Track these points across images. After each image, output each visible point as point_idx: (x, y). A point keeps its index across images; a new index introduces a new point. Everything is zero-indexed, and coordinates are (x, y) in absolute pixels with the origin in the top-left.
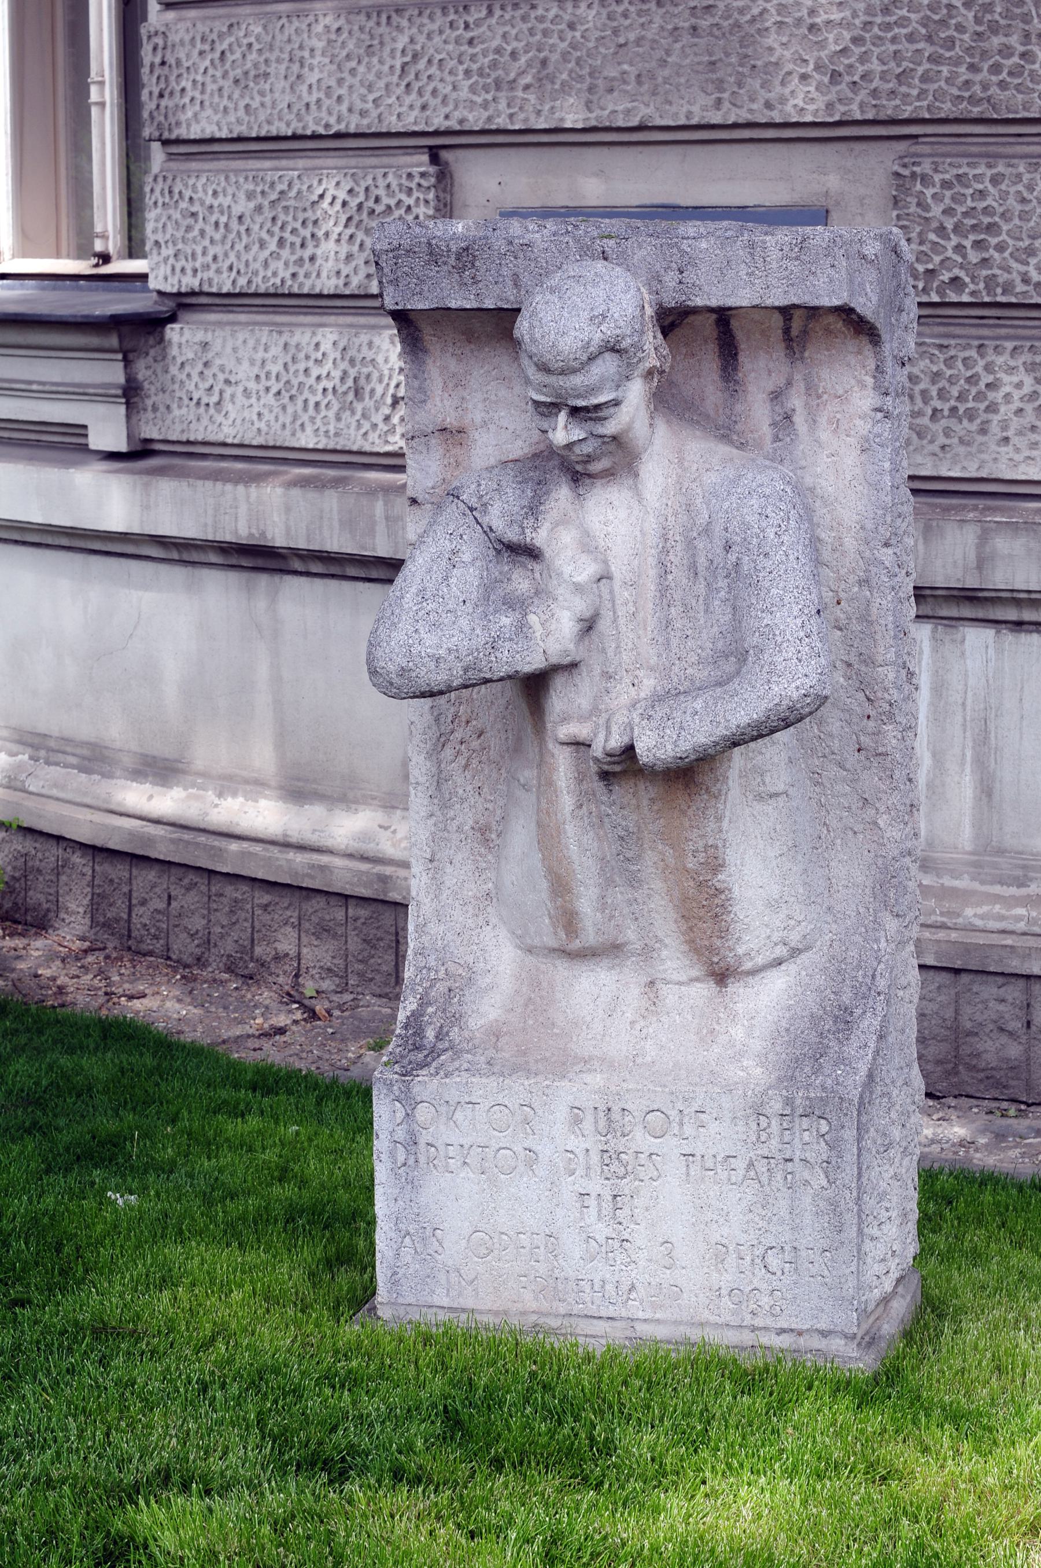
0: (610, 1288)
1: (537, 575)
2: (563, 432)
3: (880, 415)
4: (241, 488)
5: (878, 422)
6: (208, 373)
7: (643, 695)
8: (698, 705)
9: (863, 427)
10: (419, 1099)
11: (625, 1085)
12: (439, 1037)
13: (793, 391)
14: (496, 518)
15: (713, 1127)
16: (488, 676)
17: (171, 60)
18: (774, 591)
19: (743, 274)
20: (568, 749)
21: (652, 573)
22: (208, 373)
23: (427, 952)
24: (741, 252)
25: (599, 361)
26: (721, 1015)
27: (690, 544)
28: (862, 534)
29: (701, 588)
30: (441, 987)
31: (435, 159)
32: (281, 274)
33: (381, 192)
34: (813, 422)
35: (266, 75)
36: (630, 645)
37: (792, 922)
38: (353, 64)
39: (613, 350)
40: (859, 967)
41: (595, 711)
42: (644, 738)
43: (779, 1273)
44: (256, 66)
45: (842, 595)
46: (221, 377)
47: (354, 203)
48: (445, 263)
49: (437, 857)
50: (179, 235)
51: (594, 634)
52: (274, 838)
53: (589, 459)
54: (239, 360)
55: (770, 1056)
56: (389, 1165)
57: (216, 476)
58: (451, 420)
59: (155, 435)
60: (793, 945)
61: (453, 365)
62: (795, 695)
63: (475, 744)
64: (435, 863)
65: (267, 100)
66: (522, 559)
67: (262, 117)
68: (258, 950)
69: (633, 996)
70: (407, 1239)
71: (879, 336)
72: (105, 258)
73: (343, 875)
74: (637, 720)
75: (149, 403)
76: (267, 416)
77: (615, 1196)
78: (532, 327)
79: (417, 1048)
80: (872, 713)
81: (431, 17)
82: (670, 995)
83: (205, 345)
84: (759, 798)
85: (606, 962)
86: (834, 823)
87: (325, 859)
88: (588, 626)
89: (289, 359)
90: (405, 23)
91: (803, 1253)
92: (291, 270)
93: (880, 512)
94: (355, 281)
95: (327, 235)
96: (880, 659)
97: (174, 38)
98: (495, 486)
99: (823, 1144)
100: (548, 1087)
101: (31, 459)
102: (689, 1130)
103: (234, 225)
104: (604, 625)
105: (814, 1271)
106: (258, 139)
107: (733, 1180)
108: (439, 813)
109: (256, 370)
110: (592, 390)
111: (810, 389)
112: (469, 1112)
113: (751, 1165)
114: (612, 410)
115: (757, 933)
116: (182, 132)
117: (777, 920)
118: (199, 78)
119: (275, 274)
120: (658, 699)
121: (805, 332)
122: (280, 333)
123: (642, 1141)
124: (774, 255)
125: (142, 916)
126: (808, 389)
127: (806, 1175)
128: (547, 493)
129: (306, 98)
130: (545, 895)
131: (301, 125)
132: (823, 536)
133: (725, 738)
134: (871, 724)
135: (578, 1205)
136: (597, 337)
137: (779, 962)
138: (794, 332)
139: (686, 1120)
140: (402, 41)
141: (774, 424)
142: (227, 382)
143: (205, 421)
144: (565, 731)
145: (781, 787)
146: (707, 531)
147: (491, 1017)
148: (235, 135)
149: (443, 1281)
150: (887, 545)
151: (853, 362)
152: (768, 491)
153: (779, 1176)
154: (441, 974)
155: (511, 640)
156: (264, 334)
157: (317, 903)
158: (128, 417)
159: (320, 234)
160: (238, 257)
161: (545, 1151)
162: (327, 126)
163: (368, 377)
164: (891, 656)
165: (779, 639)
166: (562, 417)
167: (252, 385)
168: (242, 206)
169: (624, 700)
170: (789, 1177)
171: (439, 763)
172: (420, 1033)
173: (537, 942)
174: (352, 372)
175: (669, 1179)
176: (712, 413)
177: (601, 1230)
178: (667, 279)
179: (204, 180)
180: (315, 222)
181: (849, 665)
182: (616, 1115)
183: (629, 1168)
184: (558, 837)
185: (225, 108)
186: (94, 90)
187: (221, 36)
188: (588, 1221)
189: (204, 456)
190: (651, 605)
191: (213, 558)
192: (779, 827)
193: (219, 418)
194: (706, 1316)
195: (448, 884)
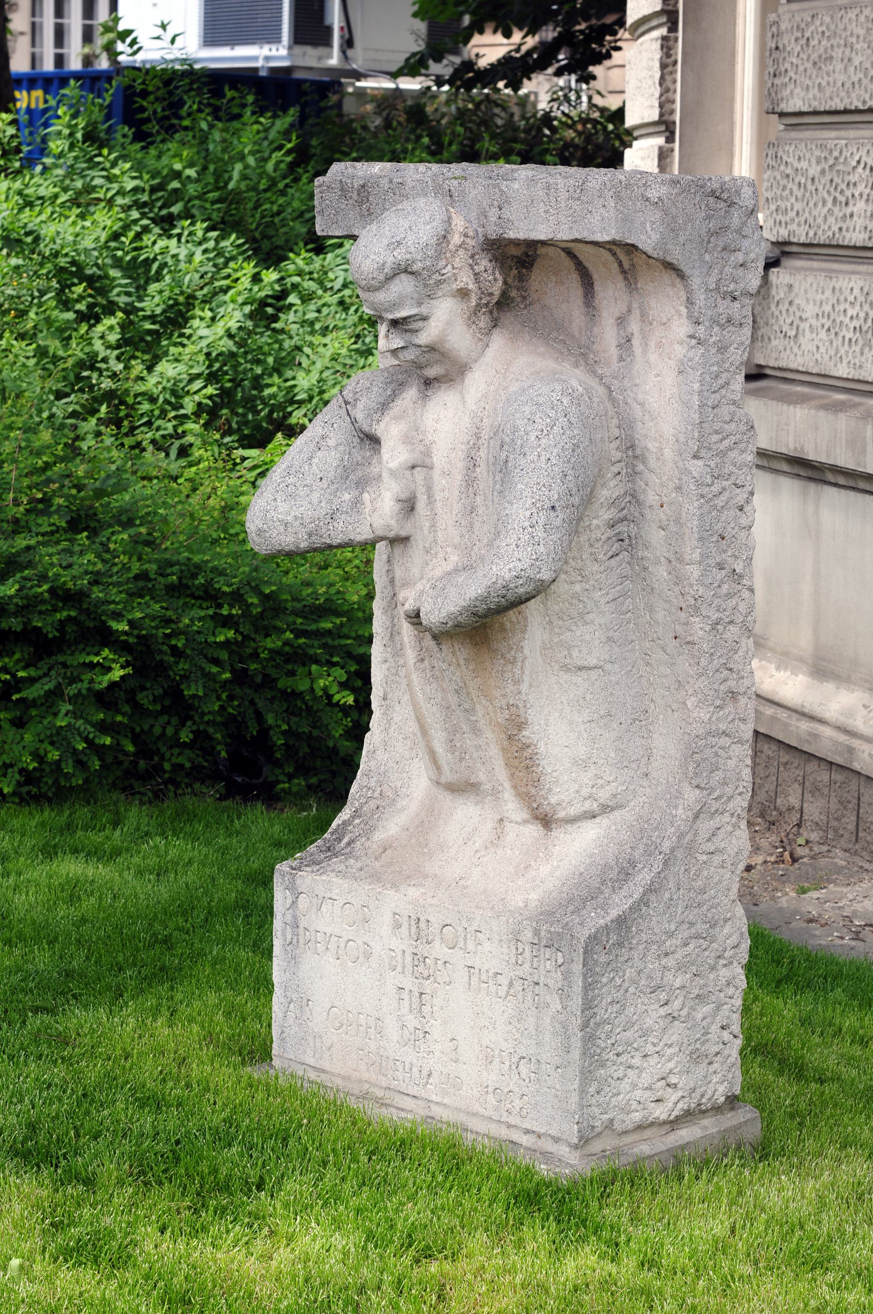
0: (415, 1070)
3: (694, 341)
5: (692, 347)
9: (680, 351)
15: (487, 945)
16: (328, 541)
18: (520, 486)
21: (460, 465)
23: (372, 774)
24: (540, 192)
25: (397, 281)
26: (541, 854)
30: (372, 804)
37: (600, 782)
39: (406, 271)
43: (527, 1080)
44: (826, 50)
45: (665, 499)
49: (389, 697)
52: (796, 708)
54: (808, 300)
60: (601, 801)
62: (507, 576)
64: (388, 702)
73: (827, 742)
76: (822, 350)
80: (684, 606)
84: (565, 668)
88: (409, 506)
89: (835, 302)
91: (543, 1066)
92: (839, 225)
93: (690, 428)
96: (687, 557)
100: (380, 893)
108: (391, 660)
110: (394, 306)
114: (420, 324)
115: (566, 786)
117: (587, 778)
118: (795, 61)
119: (830, 227)
122: (831, 278)
124: (563, 195)
131: (849, 101)
134: (683, 615)
135: (397, 996)
136: (390, 260)
137: (593, 816)
138: (626, 266)
139: (468, 936)
141: (619, 346)
142: (801, 318)
145: (593, 662)
148: (811, 110)
149: (312, 1045)
150: (696, 457)
151: (671, 293)
154: (376, 794)
155: (347, 513)
156: (821, 278)
157: (813, 766)
159: (857, 194)
160: (810, 213)
161: (377, 948)
164: (696, 556)
167: (813, 322)
168: (814, 170)
176: (576, 333)
177: (412, 1021)
178: (490, 214)
179: (793, 147)
180: (855, 184)
181: (670, 562)
182: (423, 925)
185: (808, 87)
189: (792, 381)
190: (457, 492)
191: (785, 467)
192: (588, 697)
194: (476, 1107)
195: (396, 720)
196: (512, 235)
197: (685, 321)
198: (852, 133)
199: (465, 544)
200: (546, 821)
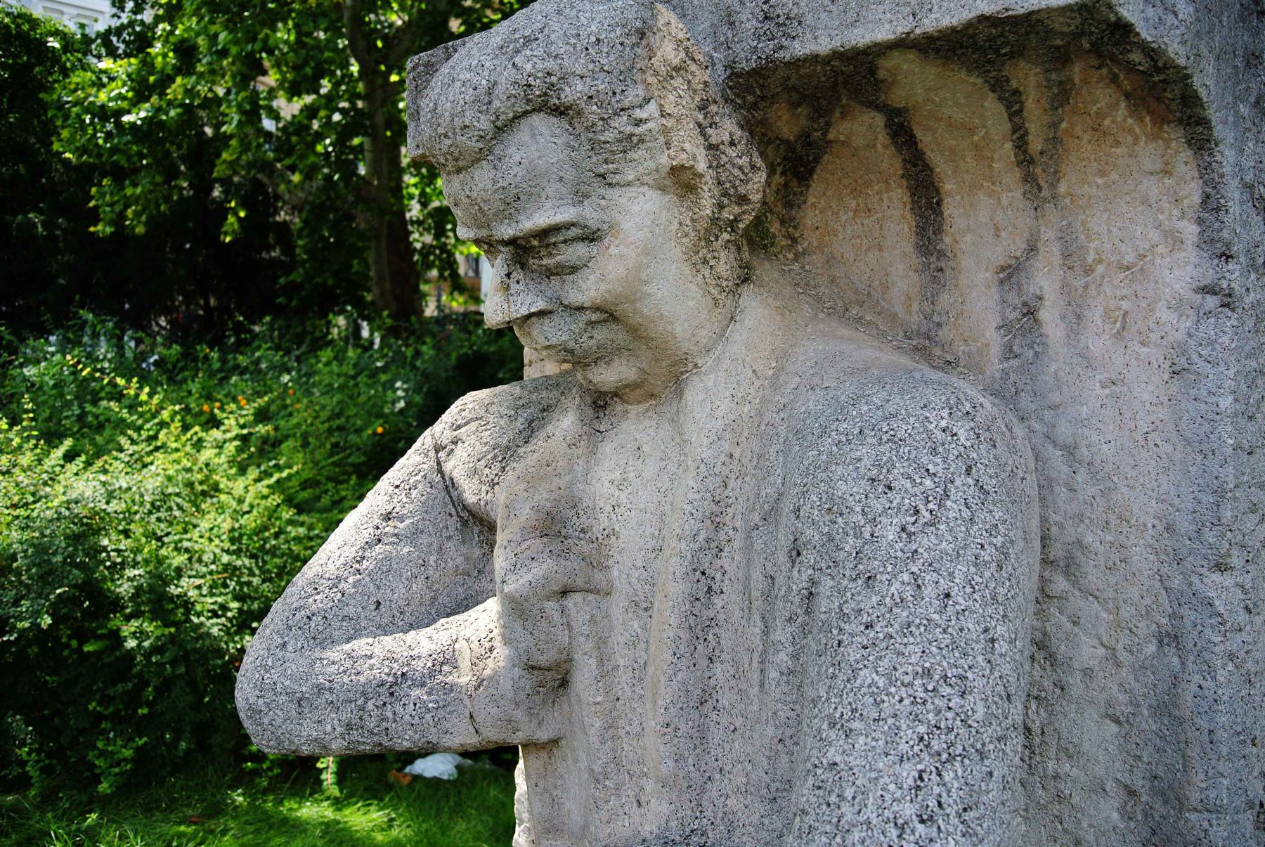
3: (1212, 302)
13: (1039, 263)
18: (866, 675)
25: (523, 133)
28: (1168, 541)
34: (1076, 319)
71: (1205, 122)
93: (1208, 499)
96: (1194, 797)
111: (1073, 257)
114: (579, 251)
126: (1066, 256)
132: (1089, 539)
136: (506, 77)
141: (1004, 326)
150: (1221, 567)
165: (848, 811)
176: (899, 310)
190: (668, 655)
197: (1190, 254)
199: (688, 777)
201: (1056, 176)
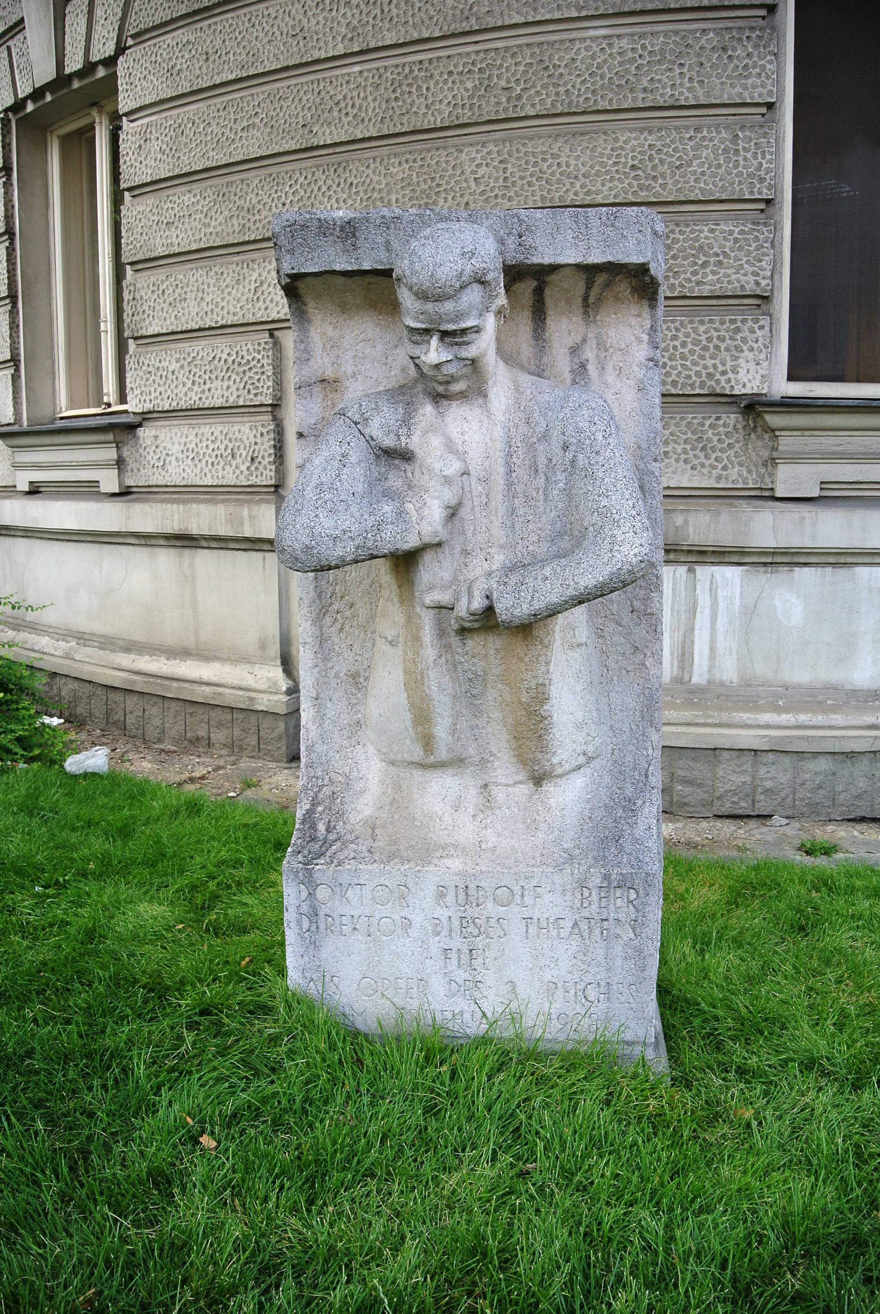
1: (409, 474)
2: (434, 353)
3: (651, 364)
4: (175, 506)
6: (158, 451)
7: (494, 567)
8: (547, 571)
10: (319, 882)
11: (478, 868)
12: (328, 831)
13: (587, 347)
14: (375, 429)
17: (138, 297)
19: (569, 237)
20: (432, 612)
21: (502, 470)
22: (158, 451)
25: (468, 290)
27: (531, 448)
29: (541, 481)
31: (272, 336)
32: (194, 398)
33: (244, 353)
34: (602, 369)
35: (185, 299)
36: (484, 529)
38: (230, 290)
40: (635, 768)
41: (455, 580)
42: (502, 600)
46: (164, 452)
47: (230, 360)
48: (332, 234)
50: (142, 383)
51: (456, 520)
53: (452, 379)
55: (583, 840)
56: (297, 931)
57: (163, 501)
58: (329, 373)
59: (132, 484)
60: (590, 755)
61: (330, 332)
63: (348, 613)
65: (186, 311)
66: (397, 462)
67: (183, 321)
68: (188, 735)
69: (472, 794)
70: (312, 984)
72: (109, 405)
73: (230, 697)
74: (495, 586)
75: (129, 468)
77: (471, 950)
78: (412, 263)
79: (313, 839)
81: (270, 262)
82: (499, 794)
83: (156, 437)
84: (572, 647)
85: (451, 771)
86: (612, 665)
87: (221, 690)
88: (453, 513)
90: (256, 266)
91: (615, 987)
93: (651, 435)
94: (231, 399)
95: (217, 378)
97: (139, 285)
98: (374, 406)
99: (631, 907)
100: (419, 871)
101: (72, 500)
102: (528, 900)
103: (170, 376)
104: (464, 512)
105: (623, 999)
106: (182, 332)
107: (562, 935)
109: (182, 448)
111: (601, 345)
112: (358, 891)
113: (576, 924)
114: (474, 336)
116: (144, 332)
120: (509, 570)
121: (599, 299)
123: (491, 908)
125: (131, 720)
127: (618, 930)
128: (415, 410)
129: (206, 309)
130: (409, 724)
133: (572, 598)
135: (443, 957)
136: (469, 268)
137: (579, 767)
138: (591, 300)
139: (526, 893)
140: (255, 275)
141: (572, 371)
142: (167, 455)
143: (157, 475)
144: (431, 598)
145: (584, 640)
146: (545, 437)
147: (367, 813)
152: (594, 406)
153: (597, 932)
154: (326, 782)
156: (185, 430)
157: (219, 711)
158: (119, 475)
159: (213, 377)
161: (417, 919)
162: (216, 322)
163: (239, 448)
166: (434, 341)
167: (180, 455)
168: (174, 366)
169: (479, 571)
170: (605, 932)
171: (321, 627)
172: (313, 827)
173: (399, 757)
174: (230, 446)
175: (513, 936)
176: (526, 364)
177: (461, 975)
182: (471, 892)
183: (482, 930)
184: (422, 680)
186: (102, 324)
187: (162, 282)
188: (450, 969)
191: (162, 542)
193: (163, 473)
195: (328, 715)
196: (536, 260)
197: (645, 346)
198: (203, 342)
200: (538, 780)
201: (597, 313)
